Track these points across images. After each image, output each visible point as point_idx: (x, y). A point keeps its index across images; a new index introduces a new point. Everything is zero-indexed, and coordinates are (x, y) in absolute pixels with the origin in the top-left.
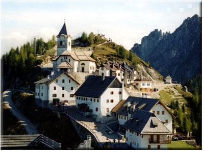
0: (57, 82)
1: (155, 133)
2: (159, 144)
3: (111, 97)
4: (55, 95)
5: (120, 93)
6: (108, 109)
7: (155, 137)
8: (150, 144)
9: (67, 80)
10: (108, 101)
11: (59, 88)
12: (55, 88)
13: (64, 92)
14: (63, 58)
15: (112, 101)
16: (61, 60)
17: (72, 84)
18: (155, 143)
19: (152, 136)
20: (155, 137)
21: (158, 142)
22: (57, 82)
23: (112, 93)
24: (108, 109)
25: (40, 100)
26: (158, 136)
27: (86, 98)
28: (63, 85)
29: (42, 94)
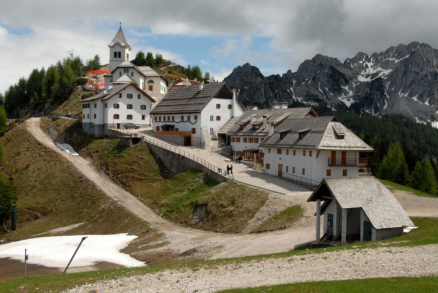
1: (338, 149)
2: (345, 168)
3: (216, 113)
4: (117, 117)
5: (230, 107)
6: (212, 129)
7: (339, 157)
8: (329, 168)
9: (135, 94)
10: (212, 118)
11: (123, 106)
13: (130, 112)
14: (122, 71)
15: (218, 118)
16: (119, 74)
17: (144, 101)
18: (339, 166)
19: (334, 153)
20: (339, 157)
21: (344, 163)
23: (218, 106)
24: (212, 129)
25: (91, 125)
26: (344, 153)
27: (171, 116)
28: (130, 102)
29: (95, 115)
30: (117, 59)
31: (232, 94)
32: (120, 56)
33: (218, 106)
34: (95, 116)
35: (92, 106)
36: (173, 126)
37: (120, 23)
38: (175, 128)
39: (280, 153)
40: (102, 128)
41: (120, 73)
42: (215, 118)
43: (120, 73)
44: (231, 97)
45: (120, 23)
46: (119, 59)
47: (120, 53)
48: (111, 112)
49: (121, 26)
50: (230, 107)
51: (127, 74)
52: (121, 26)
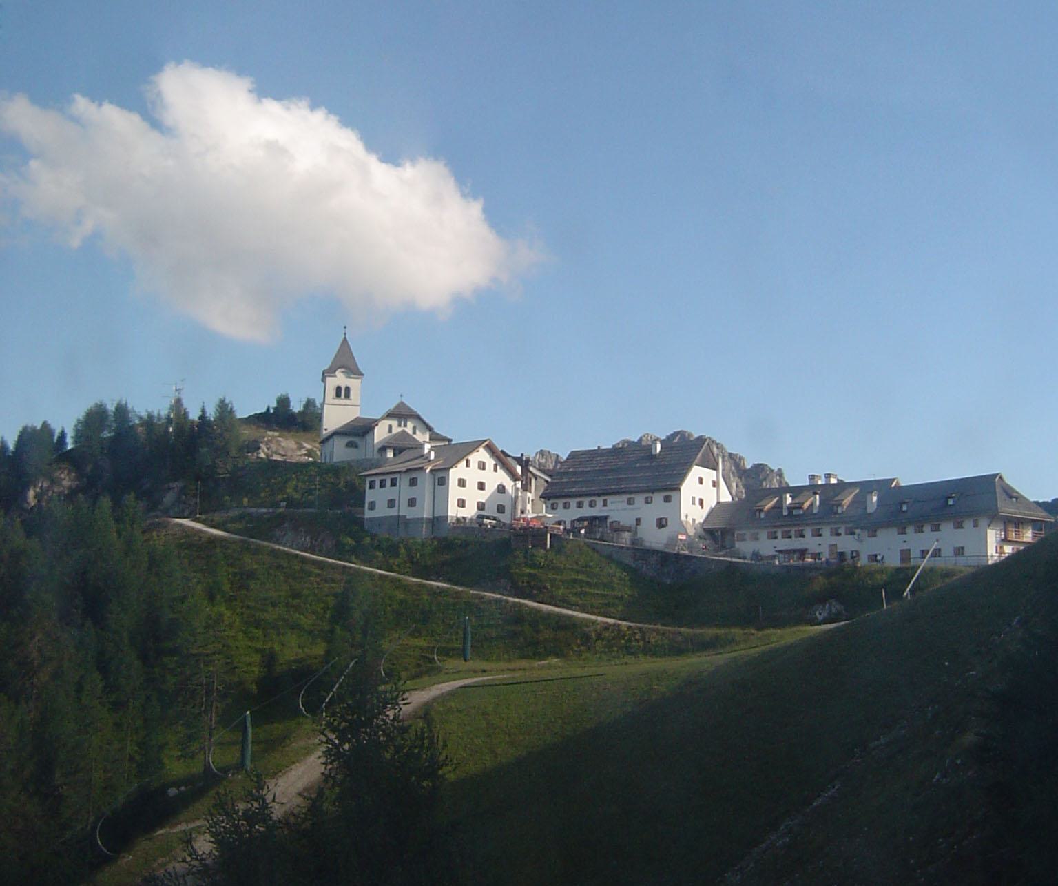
0: (468, 466)
12: (462, 483)
22: (468, 466)
30: (342, 401)
31: (718, 464)
32: (347, 396)
33: (701, 481)
34: (412, 502)
35: (404, 481)
36: (606, 518)
37: (345, 327)
38: (609, 521)
39: (902, 534)
40: (430, 525)
41: (390, 427)
42: (697, 502)
43: (390, 427)
44: (715, 468)
45: (345, 327)
46: (347, 402)
47: (348, 389)
48: (454, 492)
49: (345, 334)
50: (715, 484)
51: (405, 429)
52: (345, 334)
